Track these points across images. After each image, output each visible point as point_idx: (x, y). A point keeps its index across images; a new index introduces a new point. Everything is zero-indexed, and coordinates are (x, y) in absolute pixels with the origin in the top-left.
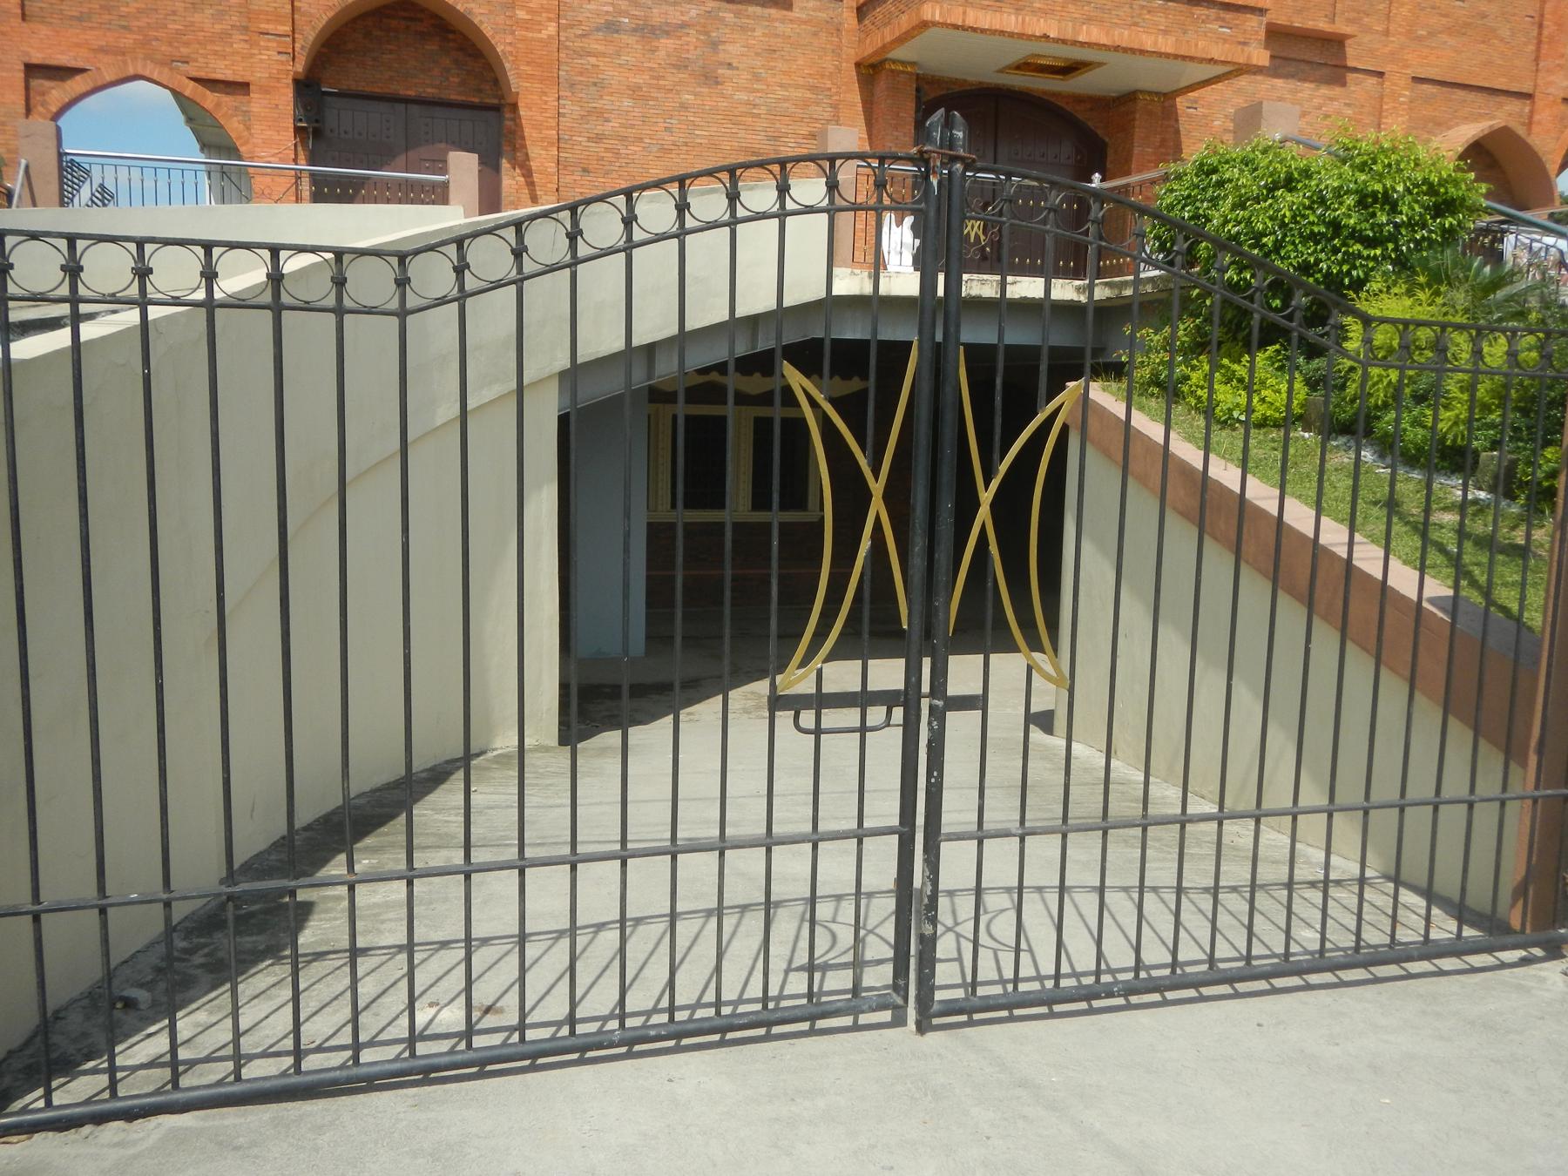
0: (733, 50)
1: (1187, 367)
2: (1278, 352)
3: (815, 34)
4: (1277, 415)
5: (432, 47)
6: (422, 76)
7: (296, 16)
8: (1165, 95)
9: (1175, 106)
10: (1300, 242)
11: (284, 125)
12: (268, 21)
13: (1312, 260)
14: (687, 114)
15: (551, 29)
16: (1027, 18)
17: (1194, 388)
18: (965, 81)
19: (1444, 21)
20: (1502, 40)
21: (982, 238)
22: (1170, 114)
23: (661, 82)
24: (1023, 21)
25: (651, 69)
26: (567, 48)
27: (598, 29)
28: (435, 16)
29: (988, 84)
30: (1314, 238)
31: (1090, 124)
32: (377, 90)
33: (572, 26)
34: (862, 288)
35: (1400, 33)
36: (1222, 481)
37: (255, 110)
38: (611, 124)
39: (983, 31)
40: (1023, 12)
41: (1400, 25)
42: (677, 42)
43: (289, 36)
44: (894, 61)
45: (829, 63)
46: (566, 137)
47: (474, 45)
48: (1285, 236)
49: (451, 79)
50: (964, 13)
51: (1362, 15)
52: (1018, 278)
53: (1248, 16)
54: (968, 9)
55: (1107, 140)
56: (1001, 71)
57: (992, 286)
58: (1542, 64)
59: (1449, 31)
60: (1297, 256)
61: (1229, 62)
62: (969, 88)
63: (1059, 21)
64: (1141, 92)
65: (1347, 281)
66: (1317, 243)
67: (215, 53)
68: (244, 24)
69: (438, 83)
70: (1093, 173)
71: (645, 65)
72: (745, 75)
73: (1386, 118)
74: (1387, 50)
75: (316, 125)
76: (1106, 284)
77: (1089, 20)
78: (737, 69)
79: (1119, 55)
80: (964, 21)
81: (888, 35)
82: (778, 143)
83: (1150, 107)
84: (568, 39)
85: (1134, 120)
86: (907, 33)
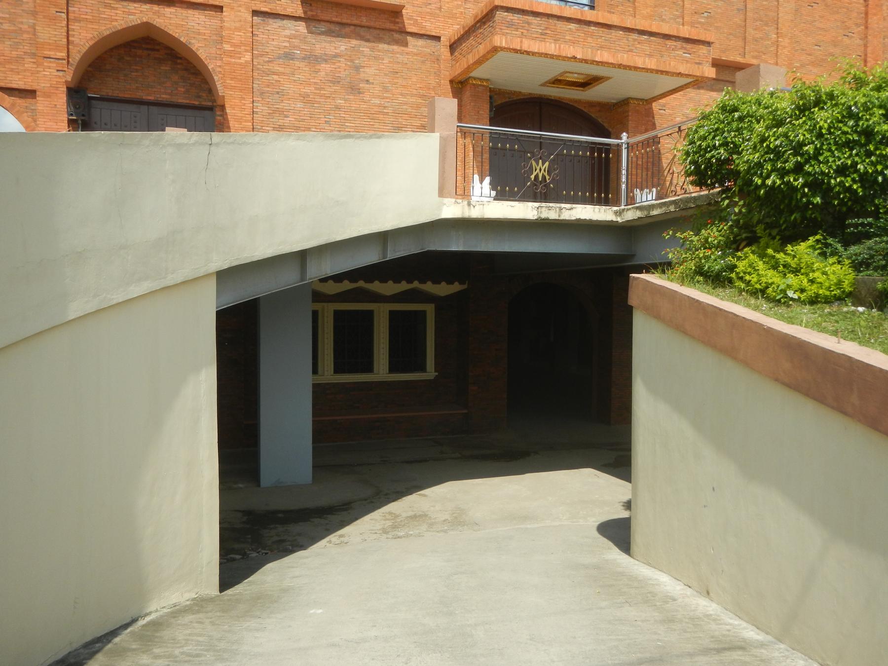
0: (369, 72)
1: (733, 258)
2: (818, 241)
3: (423, 62)
4: (828, 293)
5: (165, 68)
6: (159, 87)
7: (70, 47)
8: (646, 100)
9: (651, 108)
10: (836, 149)
11: (61, 118)
12: (50, 50)
13: (849, 162)
14: (340, 112)
15: (248, 57)
16: (562, 46)
17: (742, 274)
18: (520, 92)
19: (809, 58)
21: (547, 177)
22: (650, 114)
23: (322, 92)
24: (560, 47)
25: (315, 83)
26: (258, 69)
27: (279, 58)
28: (167, 48)
29: (534, 94)
30: (849, 145)
31: (600, 120)
32: (126, 96)
33: (262, 56)
34: (463, 213)
36: (850, 355)
37: (39, 108)
38: (289, 119)
39: (534, 54)
40: (559, 42)
42: (332, 66)
43: (65, 59)
44: (475, 79)
45: (433, 81)
46: (259, 127)
47: (195, 66)
48: (822, 144)
49: (179, 89)
50: (521, 42)
52: (574, 206)
53: (701, 46)
54: (524, 40)
55: (610, 130)
56: (544, 85)
57: (556, 211)
59: (813, 64)
60: (834, 161)
61: (690, 75)
62: (522, 97)
63: (583, 48)
64: (632, 98)
65: (880, 179)
66: (851, 149)
67: (12, 70)
68: (33, 51)
69: (170, 91)
70: (622, 133)
75: (83, 118)
76: (637, 208)
77: (602, 47)
78: (373, 84)
79: (622, 71)
80: (521, 47)
81: (471, 59)
83: (637, 108)
84: (259, 63)
85: (628, 116)
86: (484, 56)
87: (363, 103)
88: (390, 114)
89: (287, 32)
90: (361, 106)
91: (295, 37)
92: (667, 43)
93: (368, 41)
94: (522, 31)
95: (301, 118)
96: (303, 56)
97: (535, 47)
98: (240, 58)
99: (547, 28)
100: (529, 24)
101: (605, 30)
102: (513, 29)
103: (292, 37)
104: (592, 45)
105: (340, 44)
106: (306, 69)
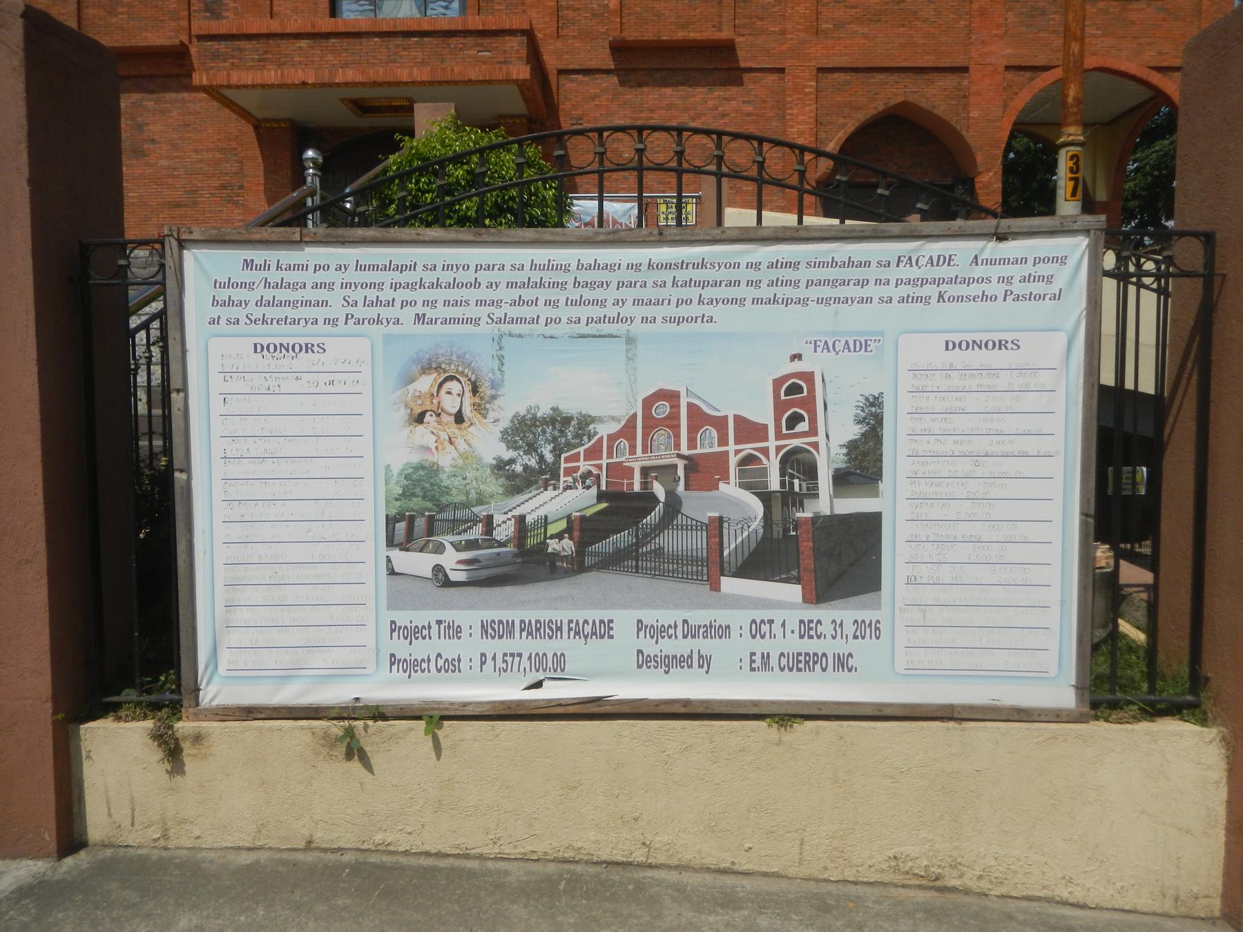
16: (286, 72)
20: (925, 20)
24: (282, 73)
35: (798, 30)
41: (798, 23)
50: (229, 75)
51: (754, 20)
53: (507, 38)
54: (232, 72)
58: (974, 37)
64: (502, 117)
73: (791, 108)
74: (784, 47)
77: (346, 65)
78: (159, 142)
80: (229, 81)
82: (196, 196)
92: (450, 42)
93: (152, 92)
94: (232, 61)
97: (247, 78)
99: (266, 52)
100: (240, 50)
101: (353, 40)
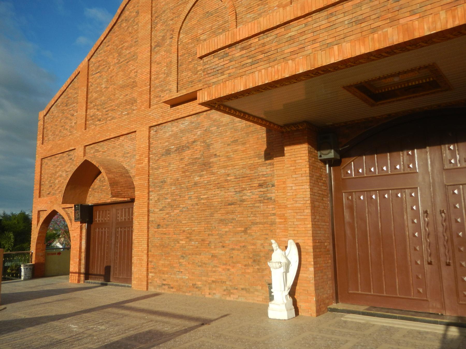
27: (163, 155)
71: (180, 167)
72: (223, 159)
78: (219, 156)
87: (212, 176)
88: (232, 180)
89: (167, 135)
90: (211, 179)
91: (171, 136)
94: (228, 72)
95: (174, 198)
96: (175, 149)
98: (142, 163)
102: (219, 75)
103: (169, 137)
104: (328, 42)
105: (196, 130)
106: (176, 158)
